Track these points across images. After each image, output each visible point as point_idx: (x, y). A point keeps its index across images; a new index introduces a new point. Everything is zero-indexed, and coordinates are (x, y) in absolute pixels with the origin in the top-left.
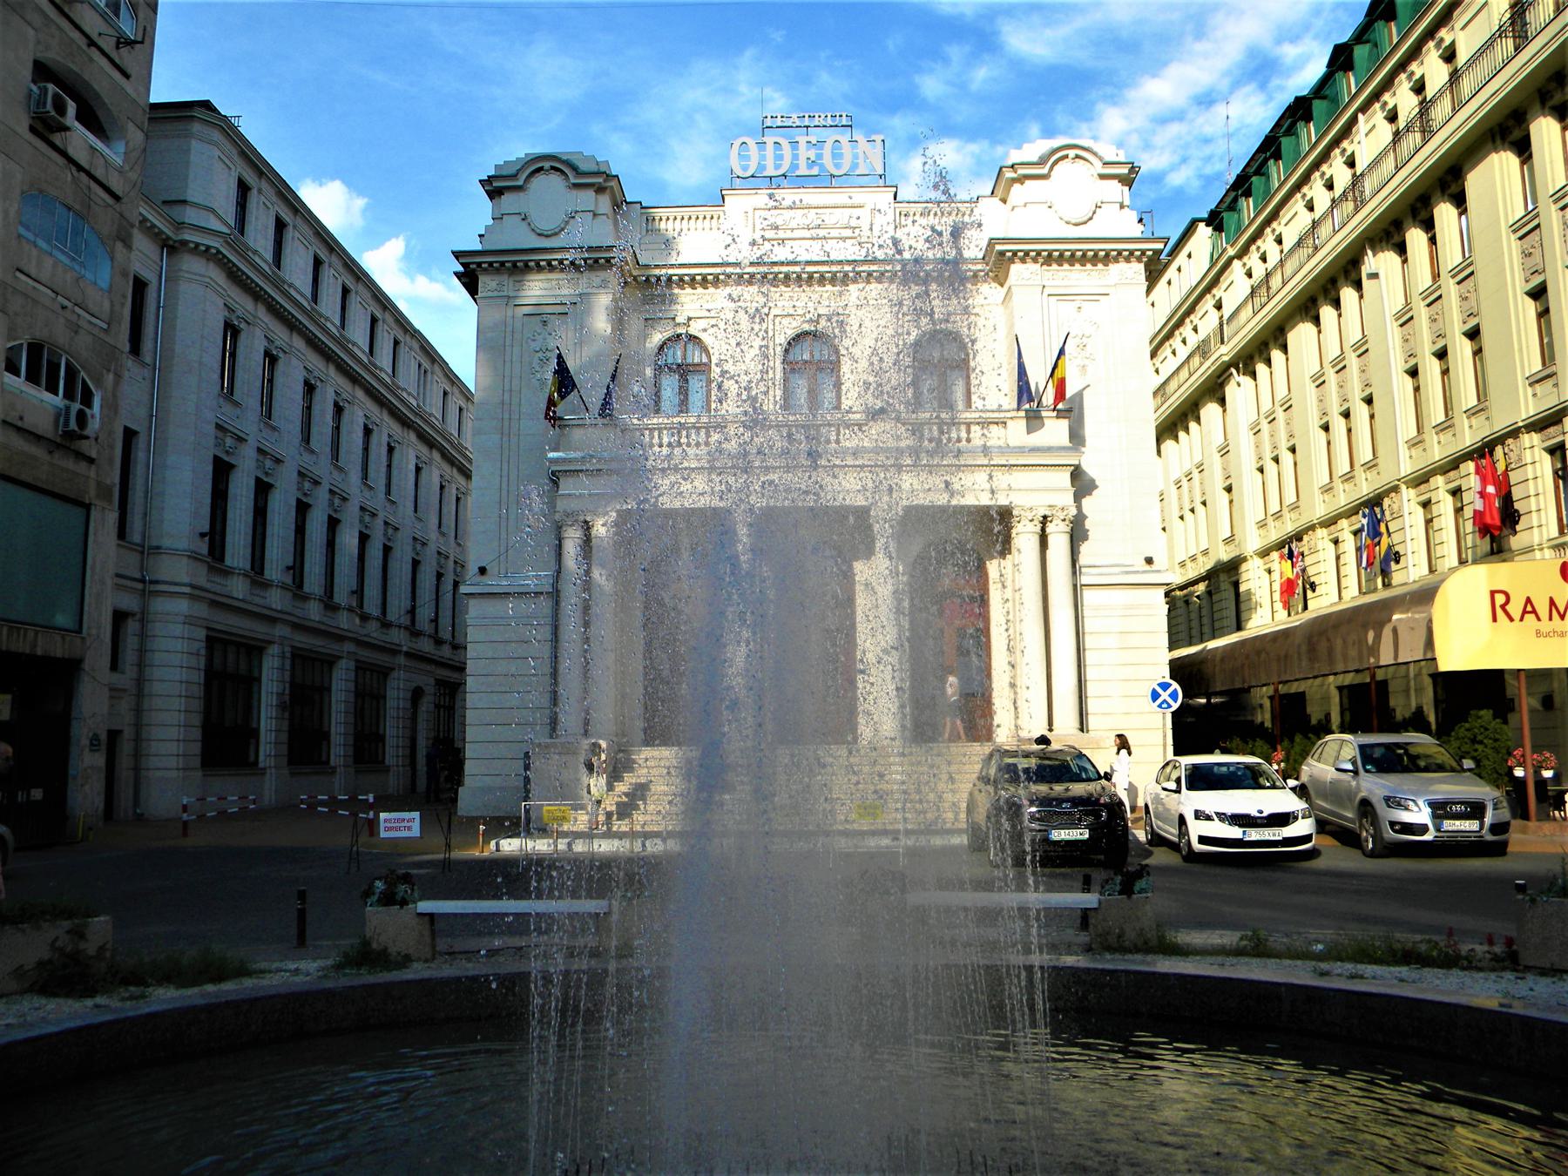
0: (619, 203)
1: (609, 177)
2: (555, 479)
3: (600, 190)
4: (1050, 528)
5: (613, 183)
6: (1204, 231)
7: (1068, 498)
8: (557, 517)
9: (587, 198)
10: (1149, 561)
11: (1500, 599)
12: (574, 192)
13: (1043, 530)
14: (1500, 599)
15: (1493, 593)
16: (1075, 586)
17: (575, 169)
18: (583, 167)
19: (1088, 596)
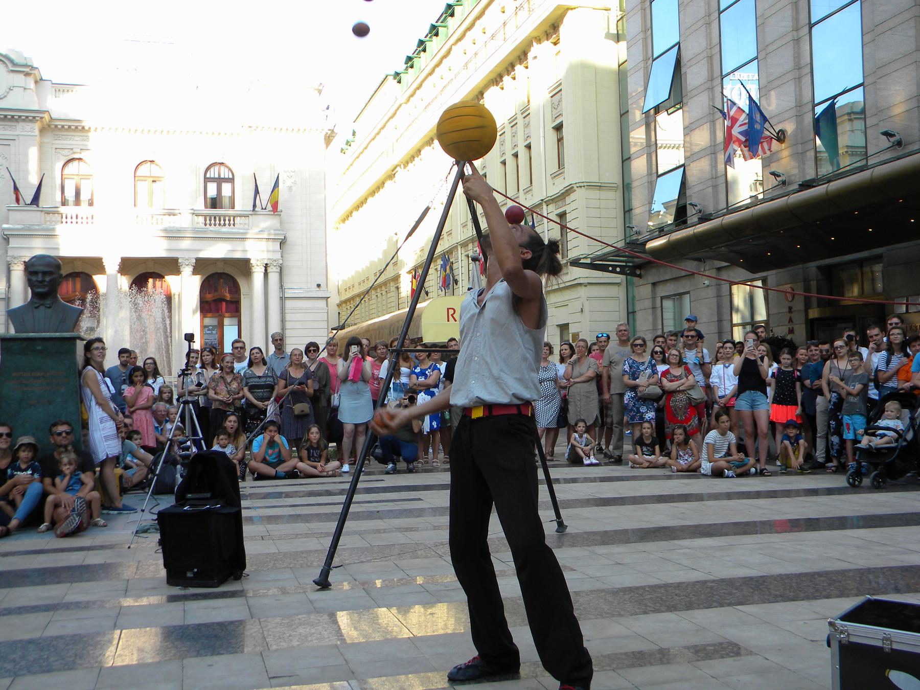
0: (39, 81)
1: (33, 68)
2: (7, 239)
3: (27, 74)
4: (269, 270)
5: (36, 72)
6: (391, 81)
7: (278, 256)
8: (8, 259)
9: (19, 79)
10: (319, 286)
11: (451, 312)
12: (12, 75)
13: (266, 270)
14: (451, 312)
15: (448, 309)
16: (281, 298)
17: (11, 61)
18: (17, 60)
19: (289, 304)
